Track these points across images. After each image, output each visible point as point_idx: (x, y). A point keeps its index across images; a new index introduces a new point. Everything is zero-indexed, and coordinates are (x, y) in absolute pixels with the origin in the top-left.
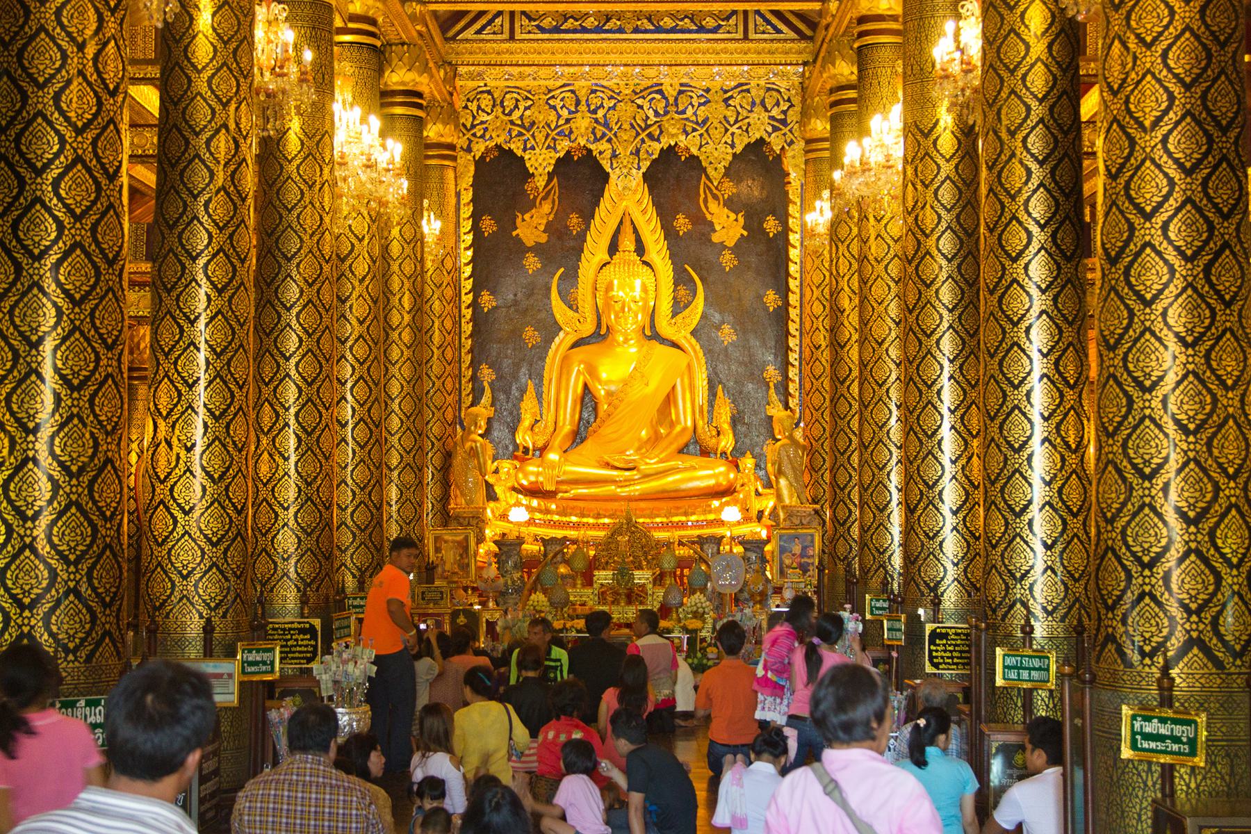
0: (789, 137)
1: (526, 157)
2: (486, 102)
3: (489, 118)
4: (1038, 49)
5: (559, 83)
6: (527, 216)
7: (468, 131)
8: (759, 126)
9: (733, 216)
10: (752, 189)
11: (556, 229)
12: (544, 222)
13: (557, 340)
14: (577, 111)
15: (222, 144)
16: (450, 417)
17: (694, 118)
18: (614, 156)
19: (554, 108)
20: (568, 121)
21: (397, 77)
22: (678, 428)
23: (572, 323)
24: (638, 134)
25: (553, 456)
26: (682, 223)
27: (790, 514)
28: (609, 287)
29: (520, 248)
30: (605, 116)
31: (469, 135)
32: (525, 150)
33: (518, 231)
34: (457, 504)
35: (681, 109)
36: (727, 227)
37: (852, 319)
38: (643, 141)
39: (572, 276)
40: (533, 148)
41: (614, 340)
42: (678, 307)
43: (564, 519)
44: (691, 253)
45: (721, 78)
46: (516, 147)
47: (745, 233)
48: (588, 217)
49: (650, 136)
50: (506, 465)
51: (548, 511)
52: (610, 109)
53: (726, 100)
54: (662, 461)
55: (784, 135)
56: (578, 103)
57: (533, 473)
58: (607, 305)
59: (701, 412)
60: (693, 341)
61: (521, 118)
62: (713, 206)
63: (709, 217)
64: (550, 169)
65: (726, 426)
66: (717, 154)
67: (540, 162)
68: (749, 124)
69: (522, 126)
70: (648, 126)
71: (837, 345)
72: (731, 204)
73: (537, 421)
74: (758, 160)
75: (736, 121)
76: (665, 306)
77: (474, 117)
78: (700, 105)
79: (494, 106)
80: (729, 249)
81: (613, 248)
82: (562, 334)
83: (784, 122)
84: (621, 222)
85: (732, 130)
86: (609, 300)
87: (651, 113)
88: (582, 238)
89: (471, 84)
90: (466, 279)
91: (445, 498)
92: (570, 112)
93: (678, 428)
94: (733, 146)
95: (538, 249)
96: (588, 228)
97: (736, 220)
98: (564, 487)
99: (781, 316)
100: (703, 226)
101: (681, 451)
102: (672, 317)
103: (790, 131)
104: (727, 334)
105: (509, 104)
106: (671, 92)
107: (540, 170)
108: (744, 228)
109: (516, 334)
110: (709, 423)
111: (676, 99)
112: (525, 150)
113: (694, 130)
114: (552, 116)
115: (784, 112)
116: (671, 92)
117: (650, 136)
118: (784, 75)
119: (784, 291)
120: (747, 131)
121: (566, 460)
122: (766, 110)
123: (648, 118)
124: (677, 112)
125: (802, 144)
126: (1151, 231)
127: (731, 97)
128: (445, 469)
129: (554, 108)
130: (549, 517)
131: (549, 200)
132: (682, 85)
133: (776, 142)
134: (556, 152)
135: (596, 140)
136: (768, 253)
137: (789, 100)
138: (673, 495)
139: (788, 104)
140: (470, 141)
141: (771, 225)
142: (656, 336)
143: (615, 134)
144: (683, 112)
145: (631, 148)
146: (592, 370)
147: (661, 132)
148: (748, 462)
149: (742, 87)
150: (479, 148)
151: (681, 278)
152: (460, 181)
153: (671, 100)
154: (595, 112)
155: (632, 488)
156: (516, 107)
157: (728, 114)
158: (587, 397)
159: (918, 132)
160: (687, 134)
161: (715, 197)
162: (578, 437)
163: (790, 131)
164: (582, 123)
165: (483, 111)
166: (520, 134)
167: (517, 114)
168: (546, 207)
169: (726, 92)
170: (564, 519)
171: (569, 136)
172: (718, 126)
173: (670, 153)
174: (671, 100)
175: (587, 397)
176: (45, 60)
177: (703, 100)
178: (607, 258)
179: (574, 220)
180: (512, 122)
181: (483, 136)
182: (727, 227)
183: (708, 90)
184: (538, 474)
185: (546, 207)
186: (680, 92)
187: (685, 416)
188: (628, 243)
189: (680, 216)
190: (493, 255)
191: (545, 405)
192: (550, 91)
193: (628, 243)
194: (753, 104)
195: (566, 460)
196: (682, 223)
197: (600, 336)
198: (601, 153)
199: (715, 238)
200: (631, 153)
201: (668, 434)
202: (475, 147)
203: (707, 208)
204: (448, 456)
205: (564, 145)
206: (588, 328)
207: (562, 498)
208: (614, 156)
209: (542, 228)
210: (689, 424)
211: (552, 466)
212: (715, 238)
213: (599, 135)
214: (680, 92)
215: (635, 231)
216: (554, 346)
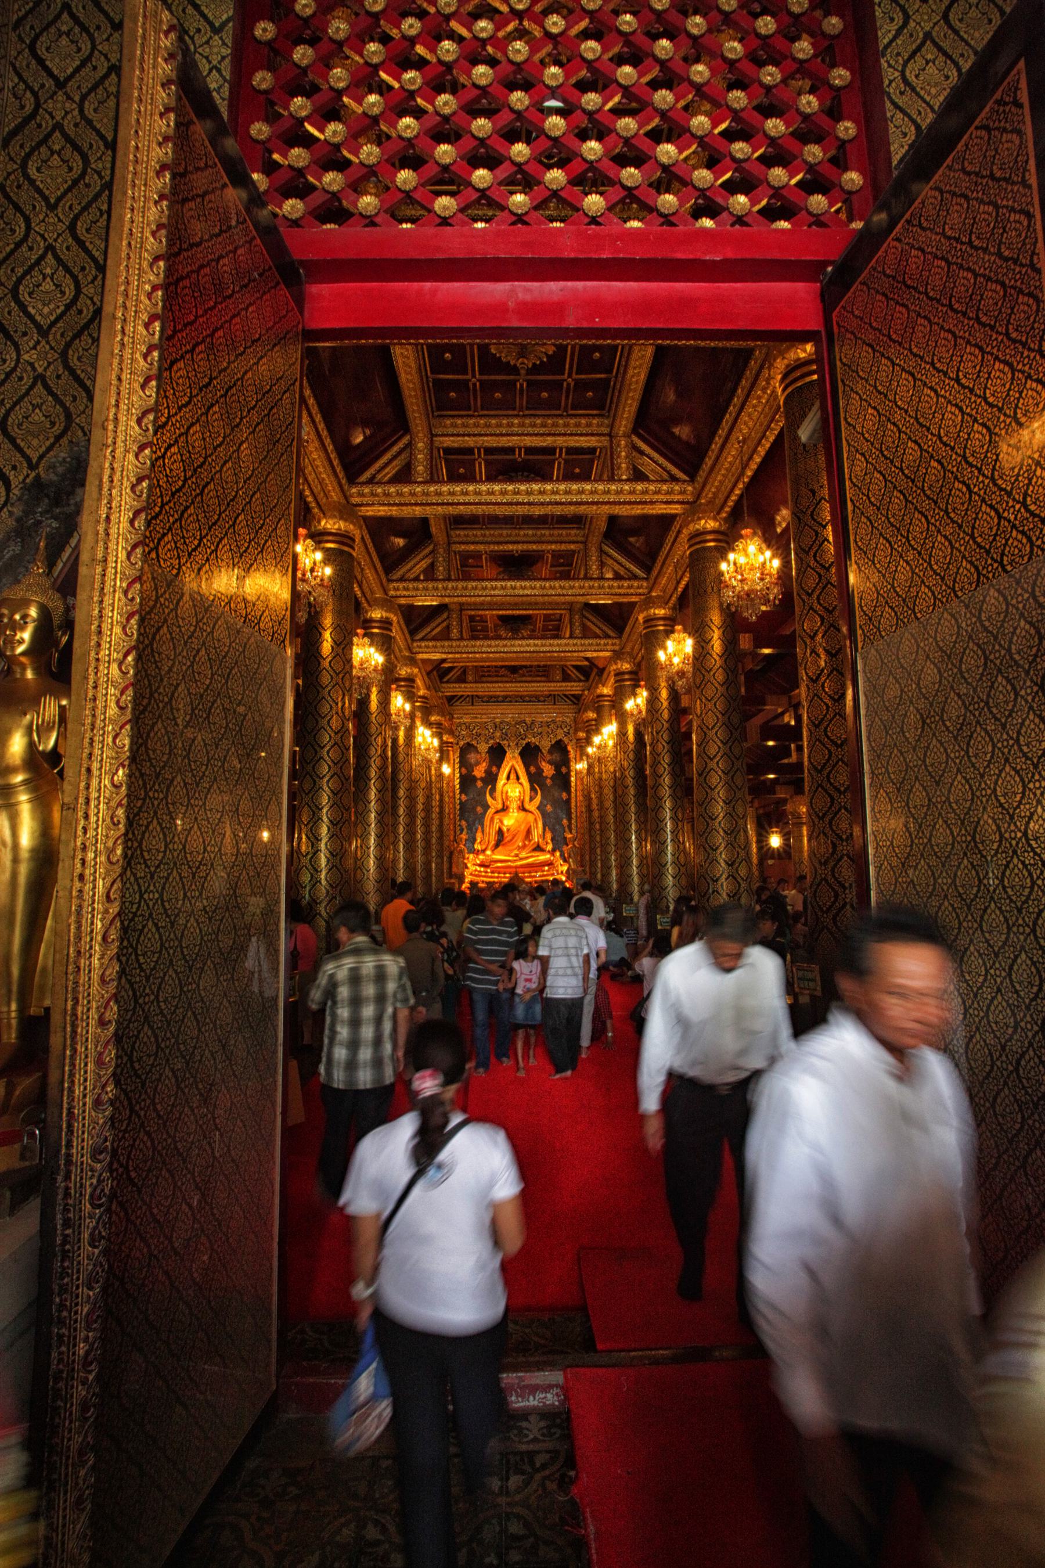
4: (665, 704)
8: (560, 735)
10: (556, 757)
11: (488, 772)
15: (380, 740)
21: (433, 718)
23: (494, 804)
25: (488, 852)
26: (532, 769)
27: (574, 871)
29: (474, 779)
34: (454, 870)
36: (548, 770)
37: (595, 802)
39: (493, 790)
42: (531, 799)
44: (536, 779)
45: (545, 718)
46: (474, 743)
48: (499, 767)
50: (471, 856)
66: (546, 744)
67: (483, 747)
71: (590, 810)
72: (550, 762)
74: (560, 747)
76: (527, 799)
81: (508, 778)
86: (507, 798)
88: (497, 775)
91: (450, 868)
95: (482, 779)
99: (568, 801)
100: (540, 771)
104: (549, 808)
109: (474, 808)
119: (569, 793)
126: (713, 765)
128: (450, 857)
133: (566, 740)
136: (563, 780)
141: (564, 770)
146: (501, 822)
148: (558, 854)
149: (554, 722)
150: (462, 743)
151: (532, 789)
152: (455, 756)
158: (500, 832)
159: (622, 733)
162: (497, 846)
164: (498, 734)
173: (528, 744)
175: (500, 832)
176: (325, 709)
179: (494, 769)
182: (548, 770)
187: (536, 837)
188: (512, 776)
190: (467, 781)
193: (512, 776)
196: (532, 769)
197: (505, 809)
204: (451, 853)
205: (491, 742)
206: (500, 806)
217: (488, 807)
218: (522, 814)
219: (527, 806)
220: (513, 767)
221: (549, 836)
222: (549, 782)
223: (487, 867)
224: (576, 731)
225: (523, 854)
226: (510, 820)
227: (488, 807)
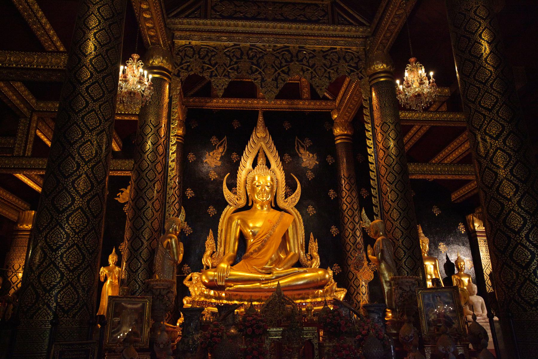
0: (360, 75)
1: (213, 80)
2: (190, 52)
3: (192, 60)
5: (232, 44)
6: (211, 154)
7: (178, 66)
9: (311, 155)
12: (220, 156)
13: (226, 210)
14: (242, 58)
16: (156, 225)
17: (307, 64)
18: (263, 80)
19: (229, 56)
20: (236, 63)
22: (292, 254)
24: (276, 71)
28: (254, 179)
30: (257, 61)
31: (179, 68)
32: (211, 76)
33: (206, 160)
35: (300, 58)
38: (279, 74)
39: (232, 186)
40: (216, 76)
41: (256, 208)
43: (230, 302)
44: (292, 170)
47: (318, 163)
49: (283, 72)
51: (220, 298)
52: (260, 58)
53: (325, 57)
54: (285, 269)
55: (357, 74)
56: (242, 54)
57: (211, 275)
58: (253, 189)
60: (296, 210)
61: (210, 60)
62: (302, 151)
63: (300, 155)
64: (226, 87)
65: (315, 254)
68: (338, 68)
69: (211, 64)
70: (282, 67)
73: (214, 252)
75: (331, 66)
76: (282, 192)
77: (182, 60)
78: (310, 58)
79: (194, 54)
80: (310, 170)
81: (254, 164)
82: (228, 207)
84: (259, 152)
85: (328, 70)
87: (283, 61)
89: (183, 42)
90: (172, 145)
92: (238, 58)
93: (292, 254)
94: (330, 78)
96: (240, 160)
97: (313, 157)
101: (293, 266)
102: (285, 199)
103: (361, 72)
104: (311, 210)
105: (203, 53)
106: (294, 52)
107: (220, 87)
108: (317, 160)
110: (307, 252)
112: (211, 76)
113: (308, 70)
114: (228, 61)
115: (356, 63)
116: (294, 52)
117: (283, 72)
118: (356, 45)
120: (337, 71)
121: (231, 268)
122: (346, 62)
123: (281, 63)
124: (297, 61)
125: (368, 78)
127: (327, 55)
129: (229, 56)
130: (221, 301)
131: (223, 146)
132: (299, 47)
134: (230, 78)
135: (253, 73)
137: (358, 57)
138: (294, 288)
139: (358, 59)
140: (179, 71)
141: (330, 160)
142: (277, 208)
143: (263, 70)
144: (302, 61)
145: (273, 77)
146: (245, 223)
147: (289, 70)
153: (294, 54)
154: (251, 59)
155: (269, 284)
156: (207, 55)
158: (242, 239)
160: (304, 72)
161: (303, 147)
163: (361, 72)
165: (188, 56)
166: (209, 68)
167: (206, 60)
168: (221, 150)
169: (324, 52)
170: (230, 302)
171: (237, 70)
172: (321, 68)
174: (294, 54)
175: (242, 239)
177: (311, 55)
178: (251, 168)
179: (234, 156)
180: (204, 63)
181: (187, 69)
183: (314, 51)
184: (215, 276)
185: (221, 150)
186: (299, 51)
189: (286, 154)
191: (219, 244)
192: (226, 48)
194: (339, 58)
195: (231, 268)
197: (248, 207)
198: (255, 79)
199: (303, 165)
200: (273, 80)
201: (285, 258)
202: (182, 75)
203: (299, 151)
206: (242, 202)
207: (229, 290)
208: (263, 80)
209: (219, 159)
210: (297, 251)
211: (223, 270)
212: (303, 165)
213: (254, 70)
214: (299, 51)
215: (266, 156)
216: (224, 213)
217: (226, 204)
218: (277, 213)
219: (281, 203)
220: (261, 148)
221: (314, 246)
222: (310, 175)
223: (221, 288)
224: (369, 62)
225: (279, 270)
226: (259, 222)
227: (226, 204)
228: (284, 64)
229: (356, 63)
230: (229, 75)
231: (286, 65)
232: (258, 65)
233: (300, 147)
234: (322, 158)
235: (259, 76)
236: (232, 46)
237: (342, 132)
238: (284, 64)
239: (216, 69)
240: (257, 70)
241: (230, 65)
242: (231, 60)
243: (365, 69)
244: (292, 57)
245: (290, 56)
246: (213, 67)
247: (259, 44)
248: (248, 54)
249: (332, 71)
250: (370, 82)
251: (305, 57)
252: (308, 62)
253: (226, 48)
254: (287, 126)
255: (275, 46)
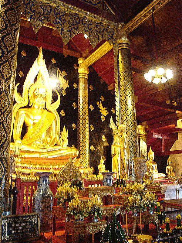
9: (65, 81)
30: (60, 17)
38: (72, 29)
48: (26, 73)
52: (61, 15)
53: (97, 26)
56: (51, 10)
59: (58, 134)
70: (73, 25)
76: (50, 99)
83: (112, 37)
92: (48, 12)
94: (99, 39)
98: (22, 154)
106: (81, 18)
110: (60, 137)
111: (82, 20)
115: (112, 35)
116: (81, 18)
117: (74, 28)
135: (56, 23)
143: (63, 24)
147: (77, 28)
154: (57, 14)
157: (97, 29)
167: (29, 6)
194: (104, 29)
206: (26, 104)
208: (62, 30)
219: (48, 107)
228: (75, 23)
229: (112, 35)
230: (42, 21)
231: (76, 25)
232: (60, 19)
233: (60, 75)
234: (71, 84)
235: (60, 27)
236: (45, 3)
237: (83, 72)
238: (75, 23)
239: (34, 14)
240: (59, 23)
241: (43, 15)
242: (44, 12)
243: (117, 40)
244: (79, 21)
245: (78, 20)
246: (33, 12)
247: (62, 7)
248: (55, 12)
249: (100, 36)
250: (118, 47)
251: (86, 23)
252: (88, 26)
253: (41, 3)
254: (53, 61)
255: (70, 11)
